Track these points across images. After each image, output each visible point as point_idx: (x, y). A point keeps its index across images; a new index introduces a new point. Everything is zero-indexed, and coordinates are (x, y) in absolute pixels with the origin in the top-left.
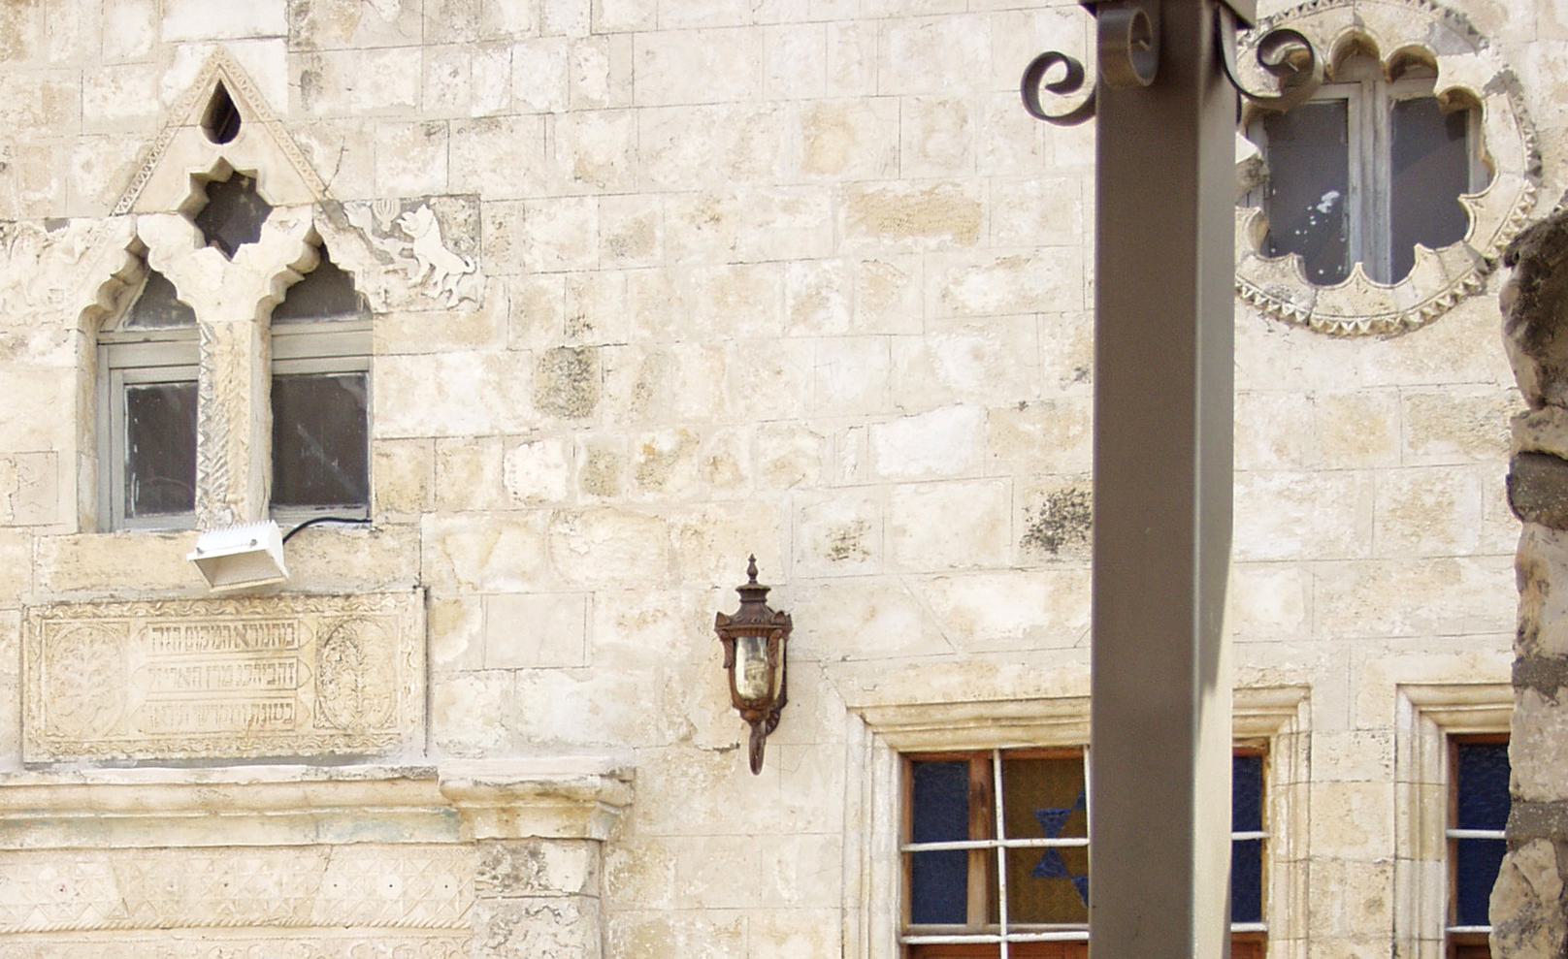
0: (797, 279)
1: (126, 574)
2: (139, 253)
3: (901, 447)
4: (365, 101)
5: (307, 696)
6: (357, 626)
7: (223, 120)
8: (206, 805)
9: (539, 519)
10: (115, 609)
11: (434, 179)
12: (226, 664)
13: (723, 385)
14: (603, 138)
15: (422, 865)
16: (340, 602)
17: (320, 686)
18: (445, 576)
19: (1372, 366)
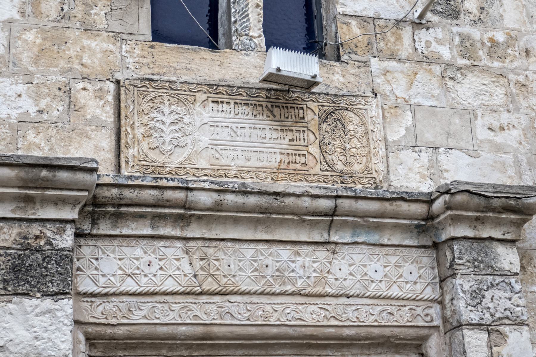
6: (345, 113)
9: (437, 69)
12: (262, 127)
13: (524, 14)
15: (393, 260)
18: (388, 93)
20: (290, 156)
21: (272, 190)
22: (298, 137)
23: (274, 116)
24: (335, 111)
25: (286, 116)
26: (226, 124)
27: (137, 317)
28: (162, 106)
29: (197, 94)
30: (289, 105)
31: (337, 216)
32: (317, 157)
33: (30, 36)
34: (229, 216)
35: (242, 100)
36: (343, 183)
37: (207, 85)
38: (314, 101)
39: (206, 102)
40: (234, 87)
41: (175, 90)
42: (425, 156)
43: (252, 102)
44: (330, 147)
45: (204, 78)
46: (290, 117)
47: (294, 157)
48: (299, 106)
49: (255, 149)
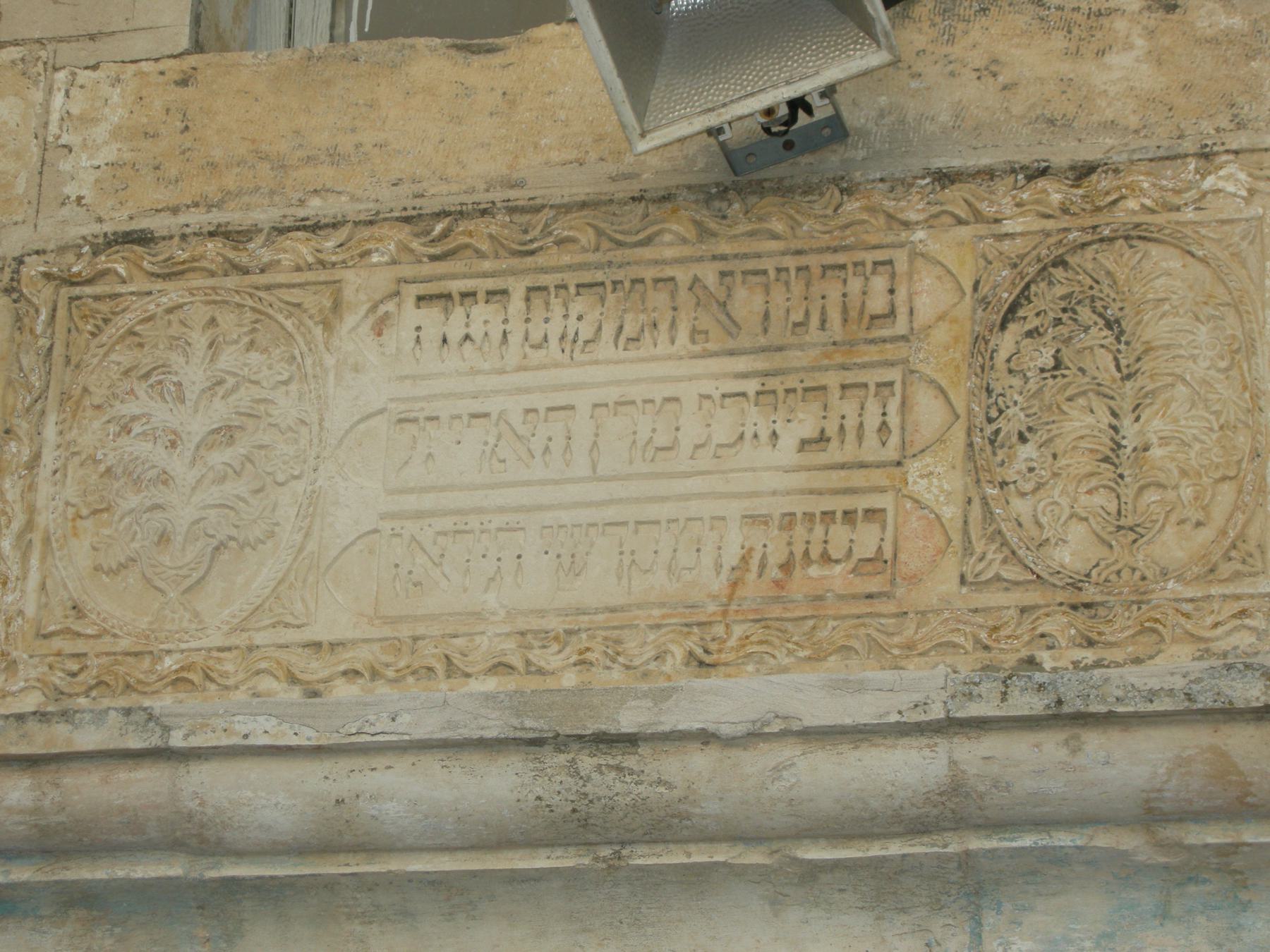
1: (335, 157)
5: (938, 483)
6: (1112, 260)
8: (577, 827)
10: (301, 247)
16: (1055, 192)
17: (986, 444)
20: (800, 531)
21: (591, 728)
22: (851, 423)
23: (732, 326)
25: (797, 316)
26: (477, 406)
28: (176, 359)
29: (349, 276)
30: (813, 261)
32: (950, 512)
34: (411, 878)
35: (570, 267)
36: (1091, 643)
37: (407, 220)
38: (960, 222)
39: (390, 306)
40: (538, 210)
41: (246, 271)
43: (620, 275)
44: (1027, 451)
45: (416, 188)
46: (815, 320)
47: (819, 530)
48: (869, 257)
49: (611, 513)
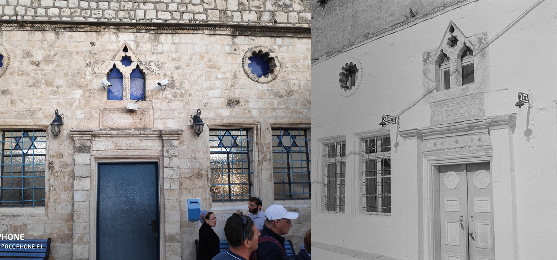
0: (199, 73)
2: (115, 65)
3: (212, 93)
4: (144, 49)
5: (138, 121)
7: (126, 50)
9: (167, 101)
11: (152, 58)
14: (174, 56)
17: (140, 120)
19: (265, 86)
24: (143, 112)
27: (103, 155)
31: (143, 134)
33: (83, 101)
42: (162, 120)
